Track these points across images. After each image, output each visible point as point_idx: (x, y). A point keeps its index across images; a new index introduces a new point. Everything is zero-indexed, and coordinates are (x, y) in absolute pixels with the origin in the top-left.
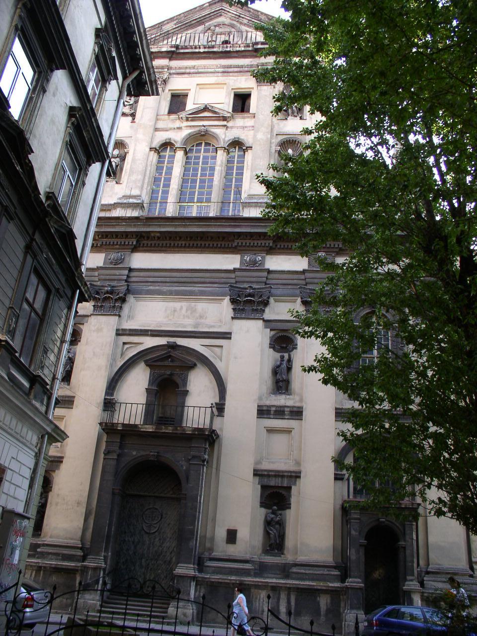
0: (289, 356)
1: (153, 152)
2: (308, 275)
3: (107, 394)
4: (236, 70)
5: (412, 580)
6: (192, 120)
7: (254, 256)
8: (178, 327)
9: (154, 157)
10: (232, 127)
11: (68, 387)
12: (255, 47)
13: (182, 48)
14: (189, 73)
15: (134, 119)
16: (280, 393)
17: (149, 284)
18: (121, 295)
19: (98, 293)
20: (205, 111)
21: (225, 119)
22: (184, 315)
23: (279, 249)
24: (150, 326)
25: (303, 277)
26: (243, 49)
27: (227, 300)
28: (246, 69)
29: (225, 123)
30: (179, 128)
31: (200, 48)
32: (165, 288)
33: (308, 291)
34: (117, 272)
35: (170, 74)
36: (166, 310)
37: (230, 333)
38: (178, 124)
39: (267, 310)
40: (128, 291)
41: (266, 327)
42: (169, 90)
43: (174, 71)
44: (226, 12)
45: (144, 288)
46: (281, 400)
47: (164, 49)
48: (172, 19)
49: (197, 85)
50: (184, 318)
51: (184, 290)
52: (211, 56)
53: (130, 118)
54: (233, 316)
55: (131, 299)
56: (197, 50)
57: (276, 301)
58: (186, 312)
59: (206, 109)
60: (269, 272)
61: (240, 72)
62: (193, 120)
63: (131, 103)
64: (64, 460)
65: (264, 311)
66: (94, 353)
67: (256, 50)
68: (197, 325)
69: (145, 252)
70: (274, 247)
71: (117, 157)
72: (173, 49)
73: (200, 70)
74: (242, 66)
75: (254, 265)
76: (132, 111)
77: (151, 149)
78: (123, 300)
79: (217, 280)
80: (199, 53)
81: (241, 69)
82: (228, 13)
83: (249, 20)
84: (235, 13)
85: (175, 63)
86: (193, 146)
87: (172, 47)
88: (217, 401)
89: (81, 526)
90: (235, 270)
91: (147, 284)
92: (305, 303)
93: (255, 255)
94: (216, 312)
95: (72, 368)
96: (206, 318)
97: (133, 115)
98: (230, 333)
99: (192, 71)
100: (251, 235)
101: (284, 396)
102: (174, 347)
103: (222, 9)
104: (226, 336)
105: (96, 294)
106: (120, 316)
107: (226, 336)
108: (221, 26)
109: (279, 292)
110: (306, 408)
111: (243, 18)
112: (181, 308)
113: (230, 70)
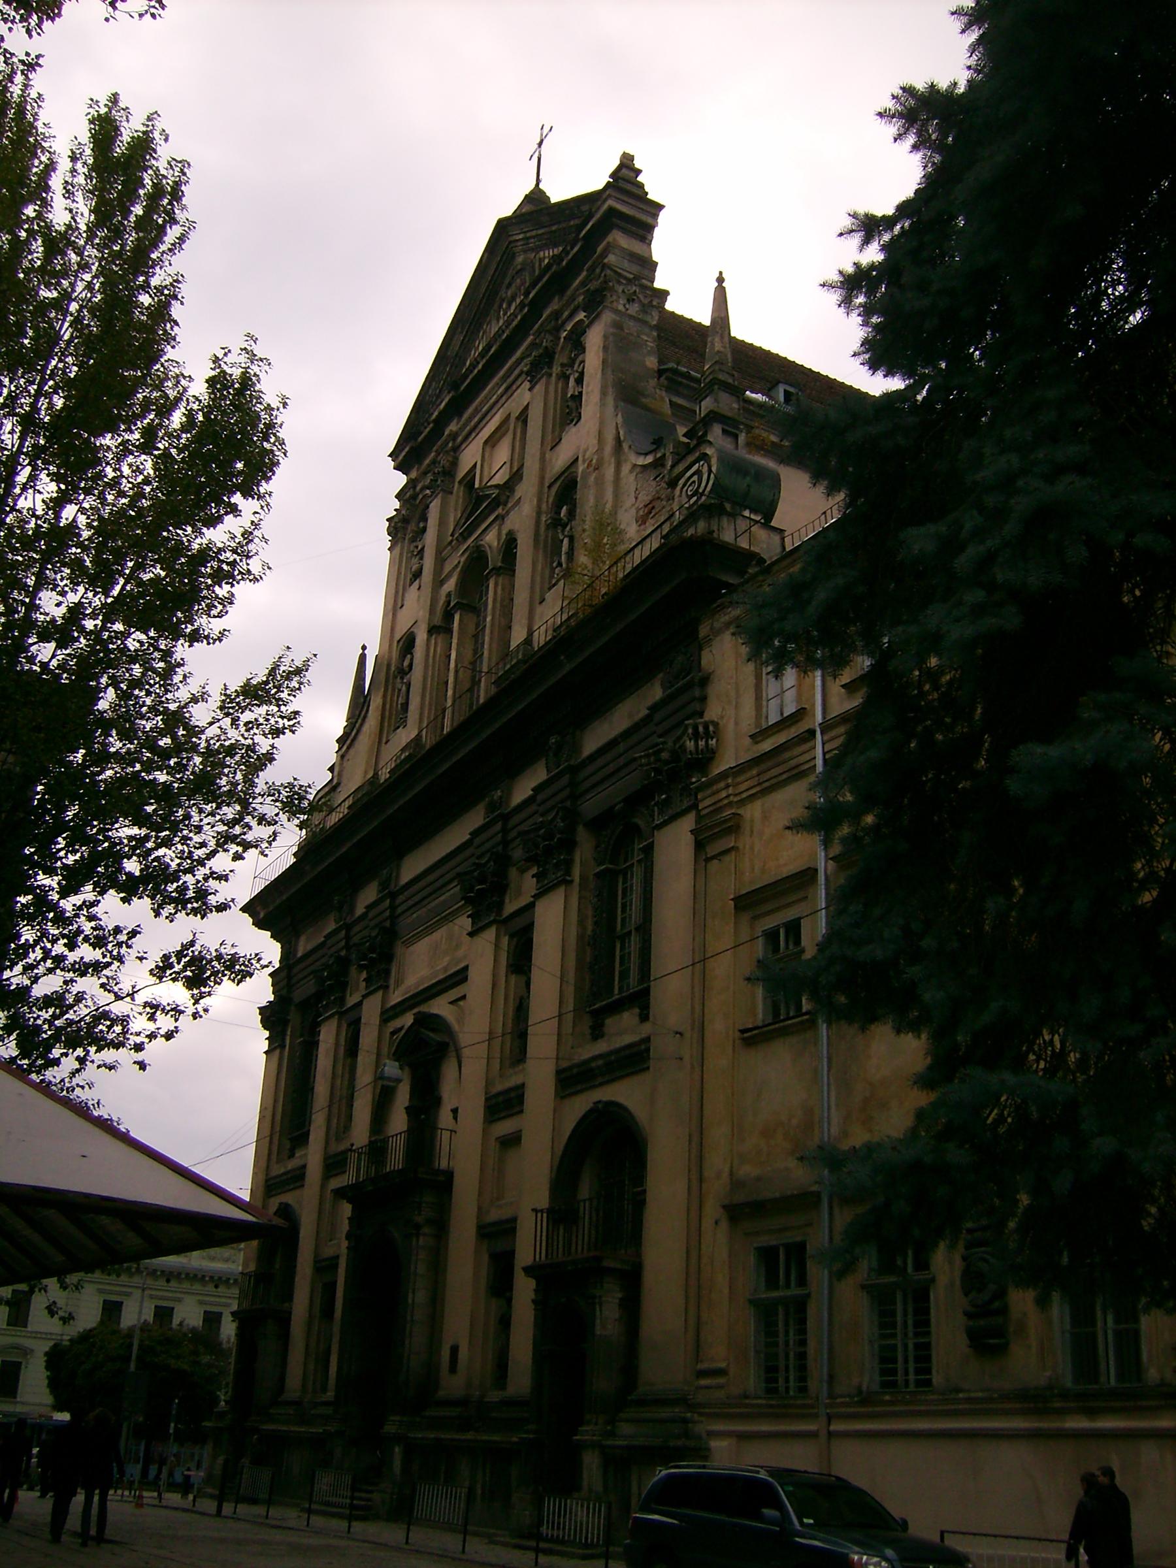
10: (508, 513)
13: (463, 383)
25: (534, 807)
37: (466, 968)
39: (507, 901)
42: (460, 482)
43: (460, 439)
49: (486, 442)
55: (399, 950)
65: (500, 905)
68: (445, 969)
73: (484, 409)
77: (432, 630)
84: (521, 236)
98: (466, 968)
103: (510, 242)
106: (387, 987)
107: (460, 977)
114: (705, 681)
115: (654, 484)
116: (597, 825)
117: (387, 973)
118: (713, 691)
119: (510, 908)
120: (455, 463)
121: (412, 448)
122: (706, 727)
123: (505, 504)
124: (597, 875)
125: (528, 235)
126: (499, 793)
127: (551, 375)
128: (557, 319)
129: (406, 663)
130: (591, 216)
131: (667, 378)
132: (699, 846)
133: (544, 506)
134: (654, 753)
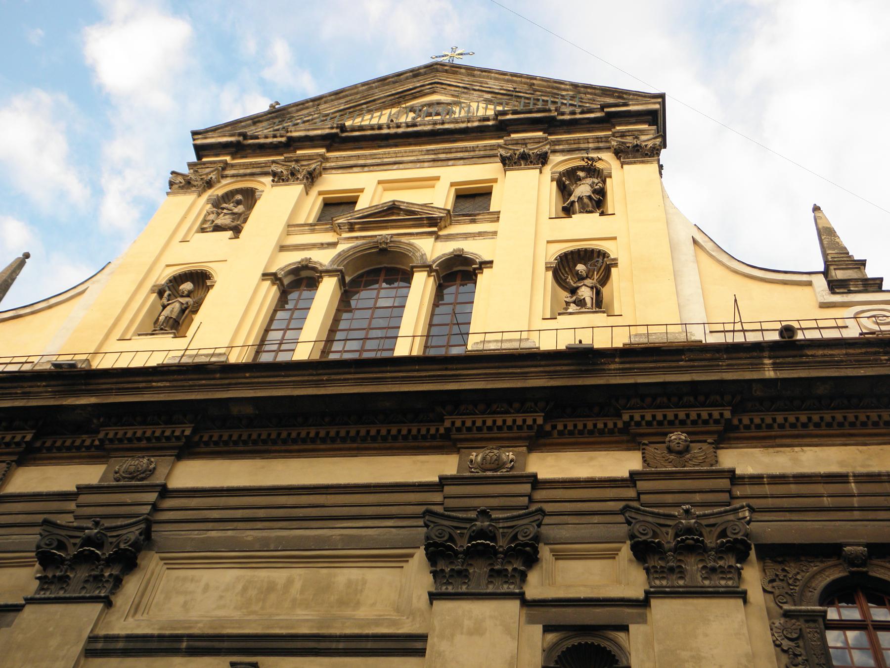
1: (268, 283)
2: (642, 485)
6: (361, 230)
7: (496, 451)
9: (270, 293)
12: (500, 118)
17: (210, 525)
18: (122, 546)
19: (61, 546)
20: (393, 214)
21: (433, 222)
22: (294, 600)
23: (561, 434)
27: (420, 554)
28: (482, 153)
29: (435, 229)
30: (334, 245)
32: (250, 535)
34: (128, 498)
35: (325, 169)
36: (245, 589)
37: (423, 638)
38: (330, 237)
41: (531, 621)
42: (320, 193)
43: (333, 164)
45: (195, 535)
49: (380, 182)
51: (302, 537)
52: (411, 140)
53: (230, 233)
54: (433, 590)
55: (152, 562)
57: (558, 556)
58: (302, 592)
59: (393, 208)
62: (365, 227)
63: (236, 210)
65: (523, 576)
69: (213, 458)
70: (548, 428)
71: (188, 296)
72: (334, 131)
78: (128, 561)
79: (394, 510)
81: (472, 154)
82: (449, 88)
87: (332, 128)
92: (643, 552)
93: (499, 448)
94: (387, 591)
97: (237, 231)
98: (423, 638)
99: (369, 161)
105: (57, 548)
109: (564, 532)
112: (290, 582)
113: (449, 156)
116: (775, 554)
117: (118, 583)
121: (238, 142)
123: (440, 229)
124: (787, 615)
129: (187, 286)
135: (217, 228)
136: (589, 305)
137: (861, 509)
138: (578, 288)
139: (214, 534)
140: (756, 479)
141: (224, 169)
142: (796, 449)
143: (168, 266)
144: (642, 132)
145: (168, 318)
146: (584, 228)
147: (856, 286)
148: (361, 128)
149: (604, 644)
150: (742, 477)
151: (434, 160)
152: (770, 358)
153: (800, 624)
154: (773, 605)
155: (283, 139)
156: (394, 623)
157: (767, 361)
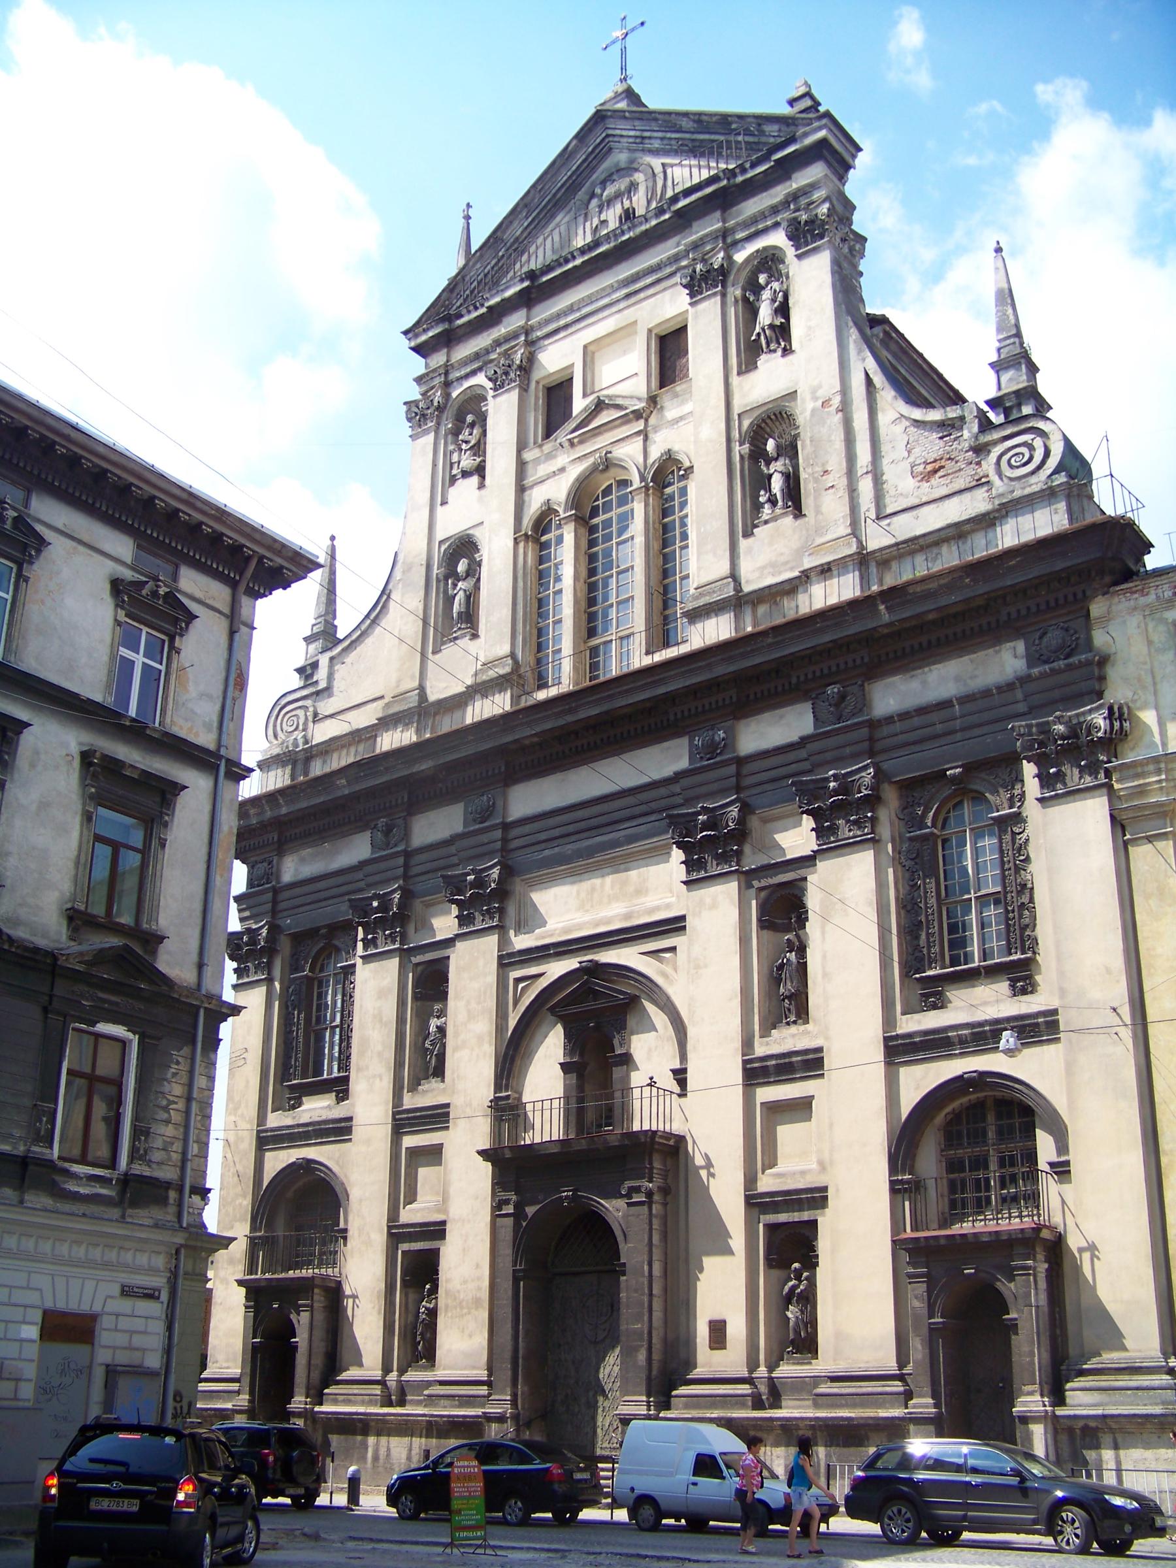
0: (797, 936)
3: (498, 1087)
4: (649, 280)
5: (1031, 1393)
6: (581, 442)
7: (711, 733)
8: (597, 925)
11: (442, 1085)
14: (566, 327)
15: (483, 477)
16: (788, 1024)
17: (543, 846)
18: (493, 885)
20: (602, 409)
21: (637, 415)
24: (552, 935)
26: (654, 222)
29: (640, 425)
30: (562, 470)
31: (574, 258)
32: (569, 848)
33: (811, 786)
34: (484, 838)
39: (747, 849)
40: (508, 872)
44: (616, 139)
46: (787, 1039)
47: (509, 293)
48: (514, 212)
50: (609, 903)
53: (475, 479)
55: (518, 885)
56: (570, 266)
57: (765, 821)
59: (600, 406)
60: (741, 761)
61: (659, 281)
62: (583, 440)
64: (448, 1227)
65: (739, 854)
66: (469, 1011)
67: (679, 213)
68: (628, 916)
72: (526, 284)
74: (658, 267)
75: (712, 752)
76: (478, 460)
80: (575, 267)
83: (662, 139)
84: (632, 133)
85: (545, 311)
86: (597, 499)
87: (522, 280)
88: (677, 1066)
89: (485, 1343)
90: (678, 776)
91: (537, 847)
95: (444, 1046)
96: (647, 890)
97: (480, 470)
98: (683, 918)
100: (694, 692)
101: (793, 1029)
102: (595, 970)
103: (608, 136)
104: (675, 925)
108: (615, 177)
110: (829, 1049)
111: (650, 138)
114: (1104, 660)
115: (941, 443)
117: (502, 911)
118: (1114, 673)
119: (751, 861)
120: (531, 359)
122: (1120, 709)
124: (911, 839)
125: (647, 134)
126: (721, 734)
127: (724, 295)
128: (724, 238)
129: (462, 567)
130: (792, 140)
131: (885, 332)
132: (1118, 823)
133: (736, 435)
134: (1038, 725)
135: (466, 474)
136: (780, 503)
137: (962, 730)
138: (770, 476)
139: (547, 853)
140: (889, 720)
141: (446, 374)
142: (926, 669)
143: (441, 542)
144: (813, 186)
145: (460, 614)
146: (769, 379)
147: (1010, 400)
148: (549, 268)
149: (796, 892)
150: (879, 721)
151: (628, 296)
152: (883, 603)
153: (917, 845)
154: (903, 830)
155: (483, 310)
156: (668, 906)
157: (882, 607)
